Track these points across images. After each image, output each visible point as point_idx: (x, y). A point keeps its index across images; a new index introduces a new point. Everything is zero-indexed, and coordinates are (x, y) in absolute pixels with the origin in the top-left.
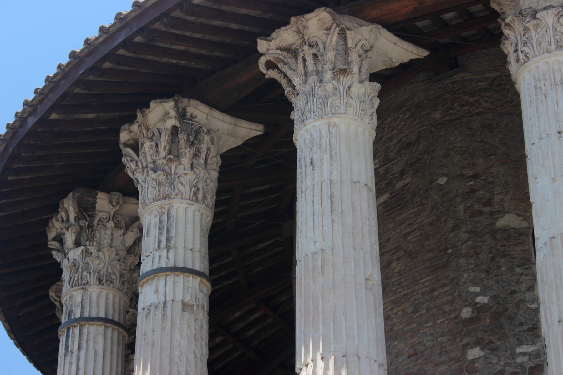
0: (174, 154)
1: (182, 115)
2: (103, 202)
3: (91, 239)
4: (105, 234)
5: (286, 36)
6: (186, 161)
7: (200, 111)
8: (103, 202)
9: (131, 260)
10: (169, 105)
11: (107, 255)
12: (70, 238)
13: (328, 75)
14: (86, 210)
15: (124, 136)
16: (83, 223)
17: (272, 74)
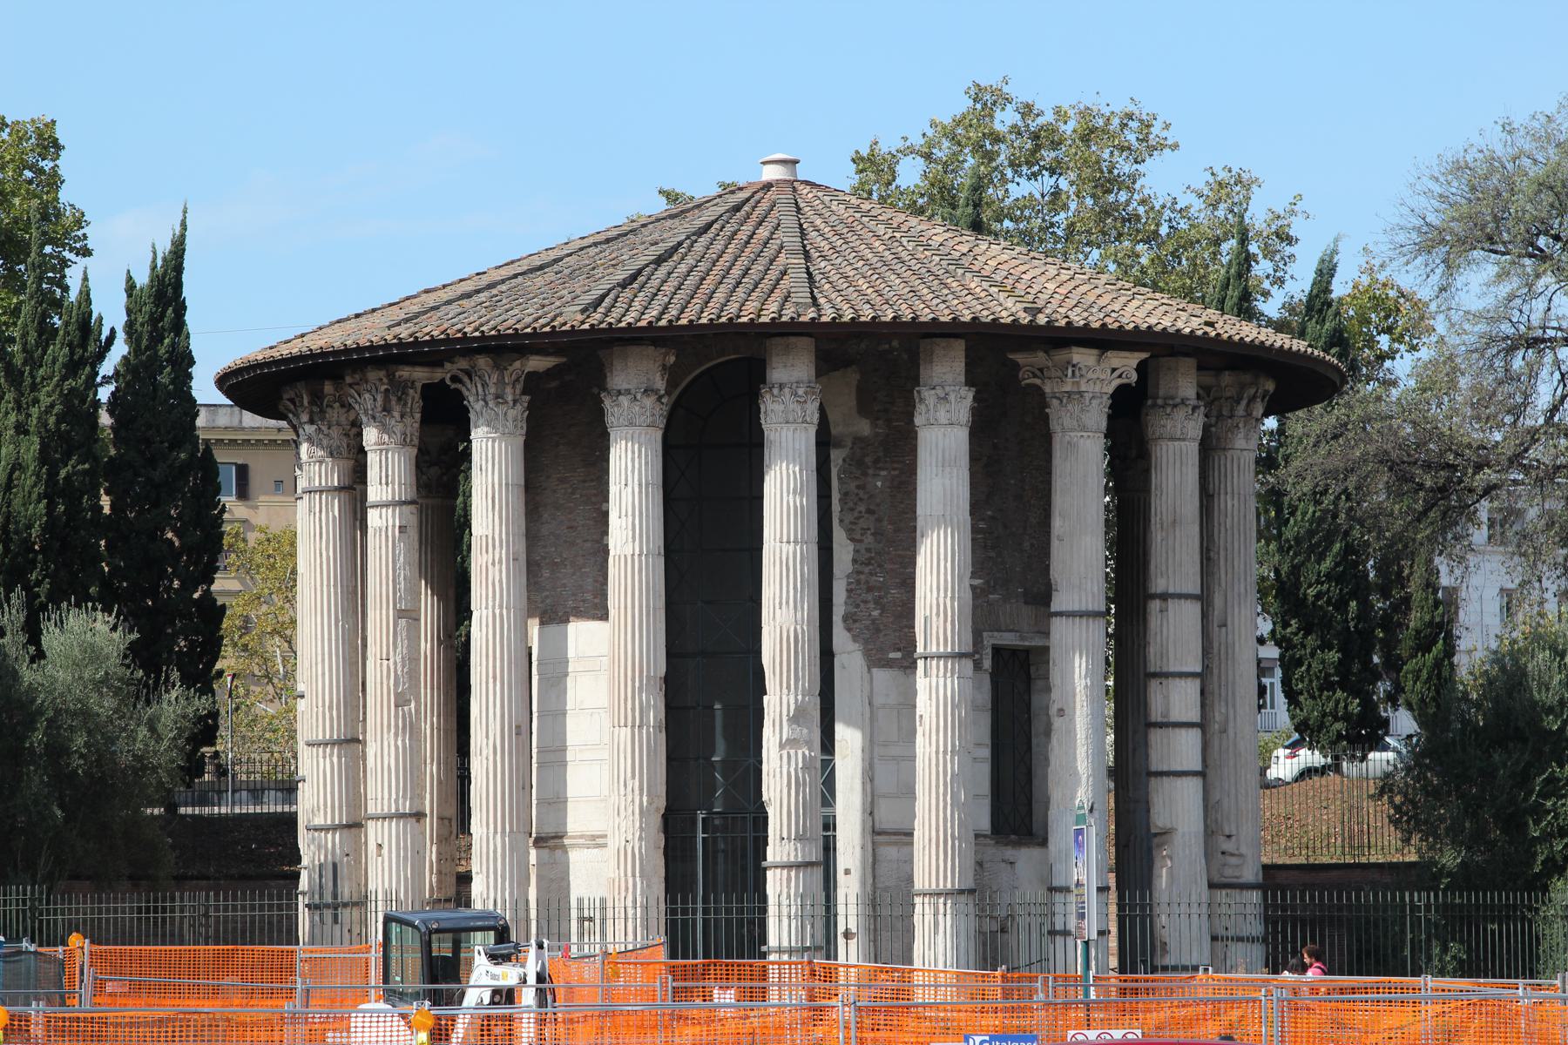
0: (387, 409)
1: (391, 377)
2: (328, 388)
3: (322, 419)
4: (335, 413)
5: (463, 364)
6: (397, 414)
7: (405, 373)
8: (328, 388)
9: (354, 431)
10: (382, 374)
11: (335, 432)
12: (305, 418)
13: (491, 404)
14: (317, 397)
15: (348, 380)
16: (316, 409)
17: (453, 386)
